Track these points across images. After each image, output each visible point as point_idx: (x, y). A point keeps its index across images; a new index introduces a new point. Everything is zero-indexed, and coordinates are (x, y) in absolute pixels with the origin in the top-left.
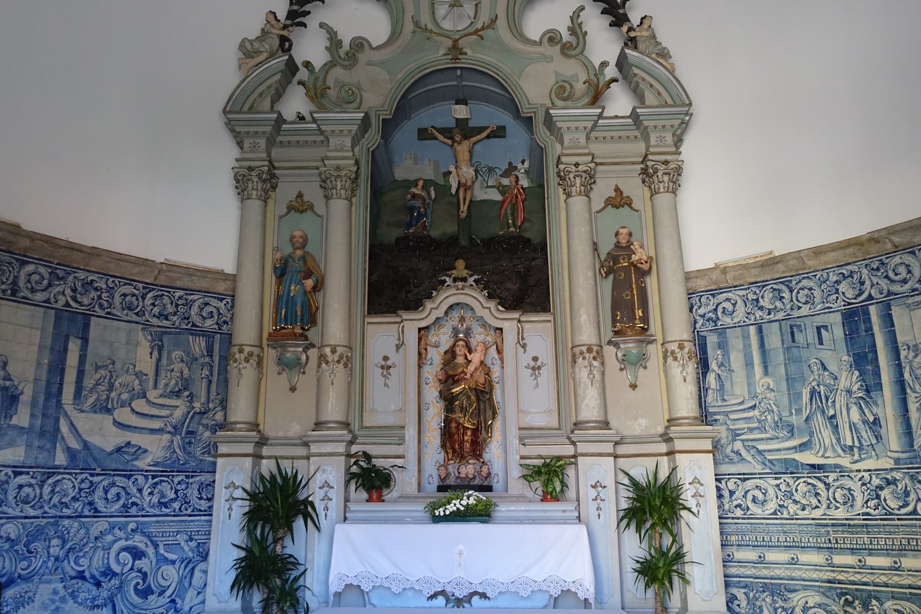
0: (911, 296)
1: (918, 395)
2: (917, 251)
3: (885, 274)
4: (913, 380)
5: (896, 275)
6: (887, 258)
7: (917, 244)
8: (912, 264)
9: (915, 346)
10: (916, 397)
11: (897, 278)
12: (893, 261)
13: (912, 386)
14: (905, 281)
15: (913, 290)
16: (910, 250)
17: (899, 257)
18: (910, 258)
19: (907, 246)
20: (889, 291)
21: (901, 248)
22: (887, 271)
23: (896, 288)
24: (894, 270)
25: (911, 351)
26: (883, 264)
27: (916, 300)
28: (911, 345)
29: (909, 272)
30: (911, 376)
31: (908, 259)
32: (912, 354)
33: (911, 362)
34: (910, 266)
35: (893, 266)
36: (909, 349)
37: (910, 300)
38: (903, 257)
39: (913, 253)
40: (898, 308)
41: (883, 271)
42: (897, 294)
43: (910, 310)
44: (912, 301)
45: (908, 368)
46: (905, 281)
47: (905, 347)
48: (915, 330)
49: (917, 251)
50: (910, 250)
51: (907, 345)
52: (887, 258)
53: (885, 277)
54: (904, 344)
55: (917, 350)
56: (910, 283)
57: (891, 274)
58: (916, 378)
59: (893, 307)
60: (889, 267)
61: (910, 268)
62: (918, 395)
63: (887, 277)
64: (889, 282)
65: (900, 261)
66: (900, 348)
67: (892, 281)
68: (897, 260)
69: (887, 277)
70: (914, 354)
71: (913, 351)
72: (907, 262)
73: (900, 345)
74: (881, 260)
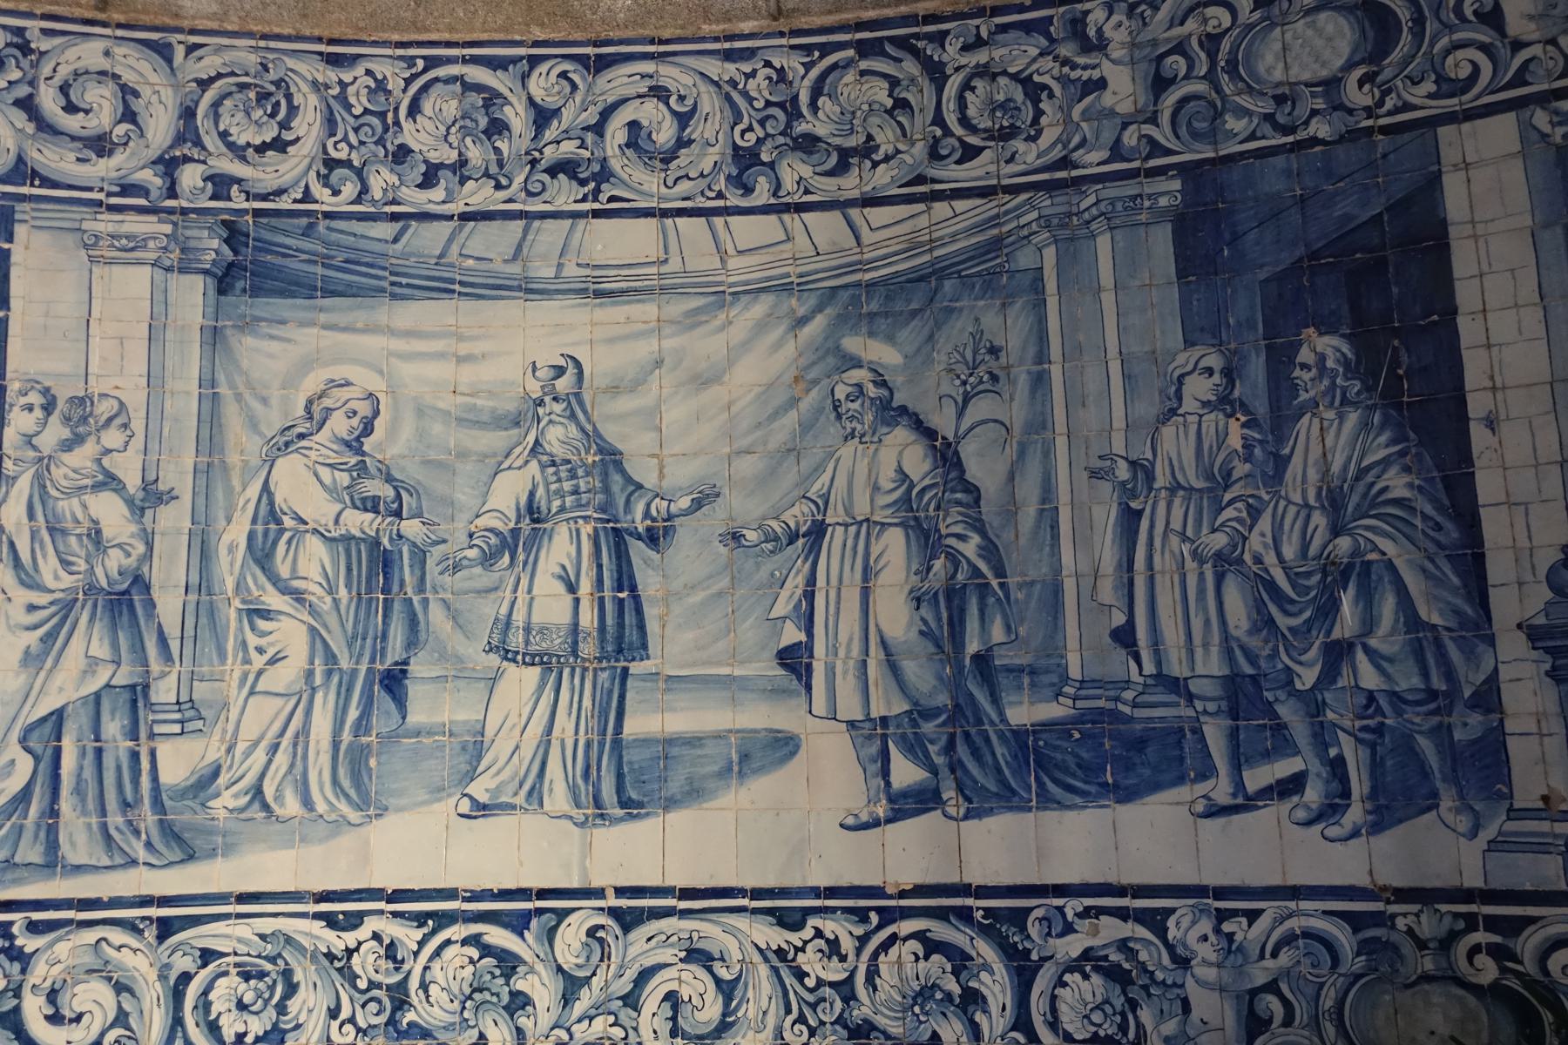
0: (113, 209)
1: (41, 599)
2: (180, 51)
3: (23, 91)
4: (34, 535)
5: (71, 108)
6: (46, 32)
7: (186, 24)
8: (146, 92)
9: (81, 401)
10: (32, 608)
11: (73, 123)
12: (71, 54)
13: (25, 556)
14: (101, 145)
15: (127, 189)
16: (154, 36)
17: (98, 46)
18: (145, 67)
19: (146, 19)
20: (20, 160)
21: (121, 18)
22: (31, 83)
23: (57, 160)
24: (64, 89)
25: (55, 419)
26: (25, 49)
27: (126, 228)
28: (63, 395)
29: (129, 116)
30: (31, 515)
31: (135, 66)
32: (55, 432)
33: (44, 464)
34: (136, 94)
35: (64, 71)
36: (48, 408)
37: (105, 224)
38: (119, 51)
39: (163, 51)
40: (41, 238)
41: (16, 75)
42: (55, 185)
43: (91, 260)
44: (111, 228)
45: (24, 485)
46: (101, 145)
47: (35, 398)
48: (95, 341)
49: (180, 51)
50: (154, 36)
51: (46, 392)
52: (45, 32)
53: (18, 103)
54: (31, 383)
55: (84, 420)
56: (118, 158)
57: (49, 101)
58: (52, 530)
59: (20, 231)
60: (46, 70)
61: (137, 105)
62: (41, 599)
63: (27, 105)
64: (30, 128)
65: (104, 64)
66: (10, 395)
67: (44, 126)
68: (90, 53)
69: (27, 105)
70: (66, 433)
71: (67, 419)
72: (128, 77)
73: (13, 387)
74: (20, 31)
